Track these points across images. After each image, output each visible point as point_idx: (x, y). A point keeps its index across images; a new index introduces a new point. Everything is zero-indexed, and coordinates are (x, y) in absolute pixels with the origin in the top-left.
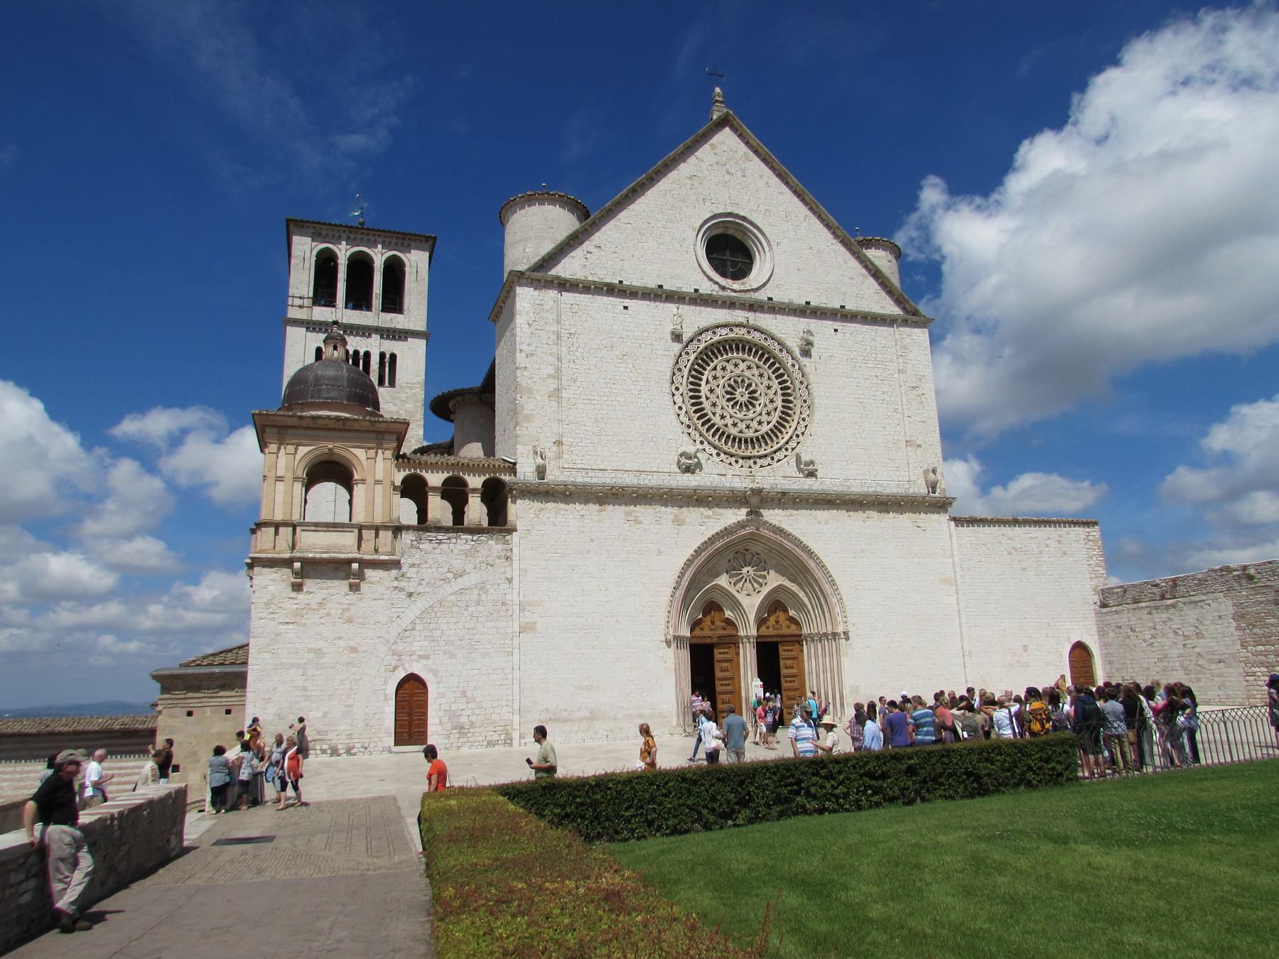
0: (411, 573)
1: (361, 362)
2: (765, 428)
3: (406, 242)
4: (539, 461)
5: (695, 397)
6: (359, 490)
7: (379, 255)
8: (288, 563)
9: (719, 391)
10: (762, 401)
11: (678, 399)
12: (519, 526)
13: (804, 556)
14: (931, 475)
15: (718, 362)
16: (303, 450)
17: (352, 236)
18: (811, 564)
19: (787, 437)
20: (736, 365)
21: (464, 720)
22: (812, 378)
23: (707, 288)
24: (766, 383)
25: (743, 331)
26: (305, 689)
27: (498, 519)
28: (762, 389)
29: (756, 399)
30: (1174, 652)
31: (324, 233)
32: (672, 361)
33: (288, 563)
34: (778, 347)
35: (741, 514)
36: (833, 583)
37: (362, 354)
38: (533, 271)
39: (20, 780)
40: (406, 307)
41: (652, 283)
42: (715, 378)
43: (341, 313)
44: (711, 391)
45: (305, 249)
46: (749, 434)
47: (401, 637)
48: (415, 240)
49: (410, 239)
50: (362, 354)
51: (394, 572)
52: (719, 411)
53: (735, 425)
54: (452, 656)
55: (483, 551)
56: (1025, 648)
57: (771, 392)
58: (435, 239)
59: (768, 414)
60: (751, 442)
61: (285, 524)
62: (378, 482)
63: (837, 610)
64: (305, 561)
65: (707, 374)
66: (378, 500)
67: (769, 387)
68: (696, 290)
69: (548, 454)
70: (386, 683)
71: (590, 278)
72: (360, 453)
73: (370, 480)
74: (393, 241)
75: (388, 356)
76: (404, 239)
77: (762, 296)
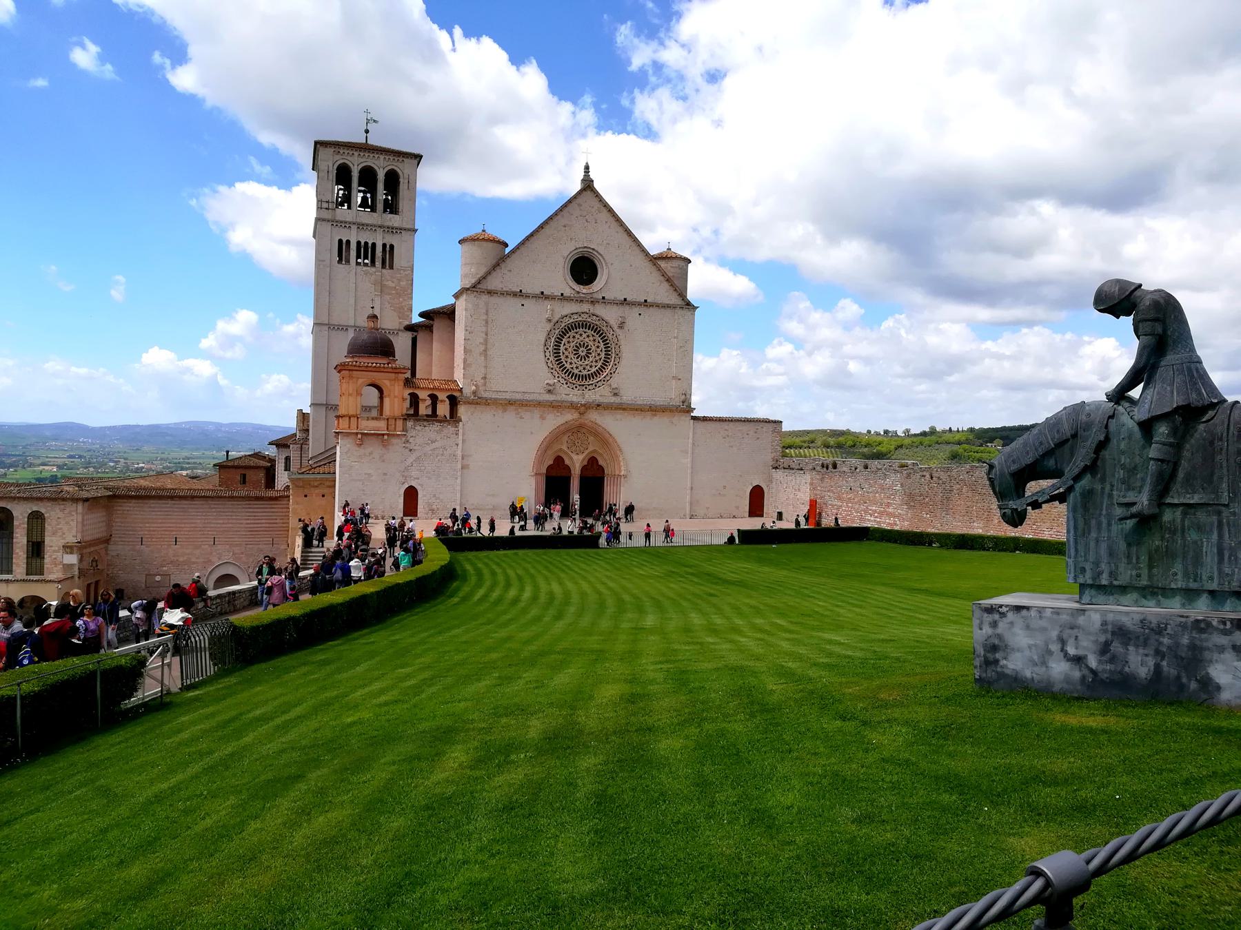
0: (411, 440)
2: (594, 370)
3: (401, 159)
5: (557, 353)
6: (387, 401)
7: (381, 169)
8: (357, 434)
10: (593, 355)
11: (548, 354)
12: (463, 418)
13: (608, 435)
14: (684, 396)
15: (571, 334)
16: (360, 381)
17: (362, 154)
19: (605, 374)
20: (581, 335)
21: (434, 507)
22: (622, 342)
23: (567, 292)
24: (597, 344)
25: (587, 316)
26: (364, 490)
27: (453, 416)
28: (593, 348)
29: (591, 354)
30: (792, 496)
31: (341, 152)
32: (545, 335)
34: (605, 324)
35: (576, 415)
36: (620, 450)
37: (370, 245)
38: (474, 287)
39: (205, 519)
40: (400, 210)
41: (538, 292)
42: (569, 342)
43: (354, 212)
44: (566, 349)
46: (585, 372)
47: (406, 469)
48: (407, 157)
49: (403, 157)
50: (370, 245)
51: (404, 439)
52: (569, 360)
53: (577, 368)
54: (430, 478)
55: (445, 431)
56: (725, 487)
57: (599, 350)
58: (422, 156)
59: (596, 361)
60: (585, 377)
61: (354, 416)
62: (395, 397)
63: (622, 464)
64: (362, 434)
66: (396, 405)
67: (598, 347)
68: (562, 294)
69: (480, 384)
70: (399, 489)
71: (505, 289)
72: (387, 383)
73: (392, 394)
74: (392, 158)
75: (388, 246)
76: (399, 156)
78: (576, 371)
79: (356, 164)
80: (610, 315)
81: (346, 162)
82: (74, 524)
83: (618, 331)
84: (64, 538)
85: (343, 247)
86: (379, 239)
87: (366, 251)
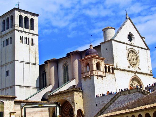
1: (27, 40)
2: (135, 63)
4: (117, 65)
8: (97, 76)
9: (131, 57)
15: (130, 53)
18: (141, 82)
23: (129, 43)
26: (100, 92)
27: (113, 72)
33: (97, 76)
35: (134, 75)
37: (28, 38)
43: (23, 29)
45: (17, 14)
46: (134, 64)
50: (28, 38)
58: (39, 15)
65: (129, 55)
77: (134, 45)
78: (132, 63)
79: (24, 15)
80: (137, 49)
81: (21, 14)
82: (12, 106)
83: (138, 54)
84: (9, 111)
85: (21, 38)
86: (30, 37)
87: (27, 40)
